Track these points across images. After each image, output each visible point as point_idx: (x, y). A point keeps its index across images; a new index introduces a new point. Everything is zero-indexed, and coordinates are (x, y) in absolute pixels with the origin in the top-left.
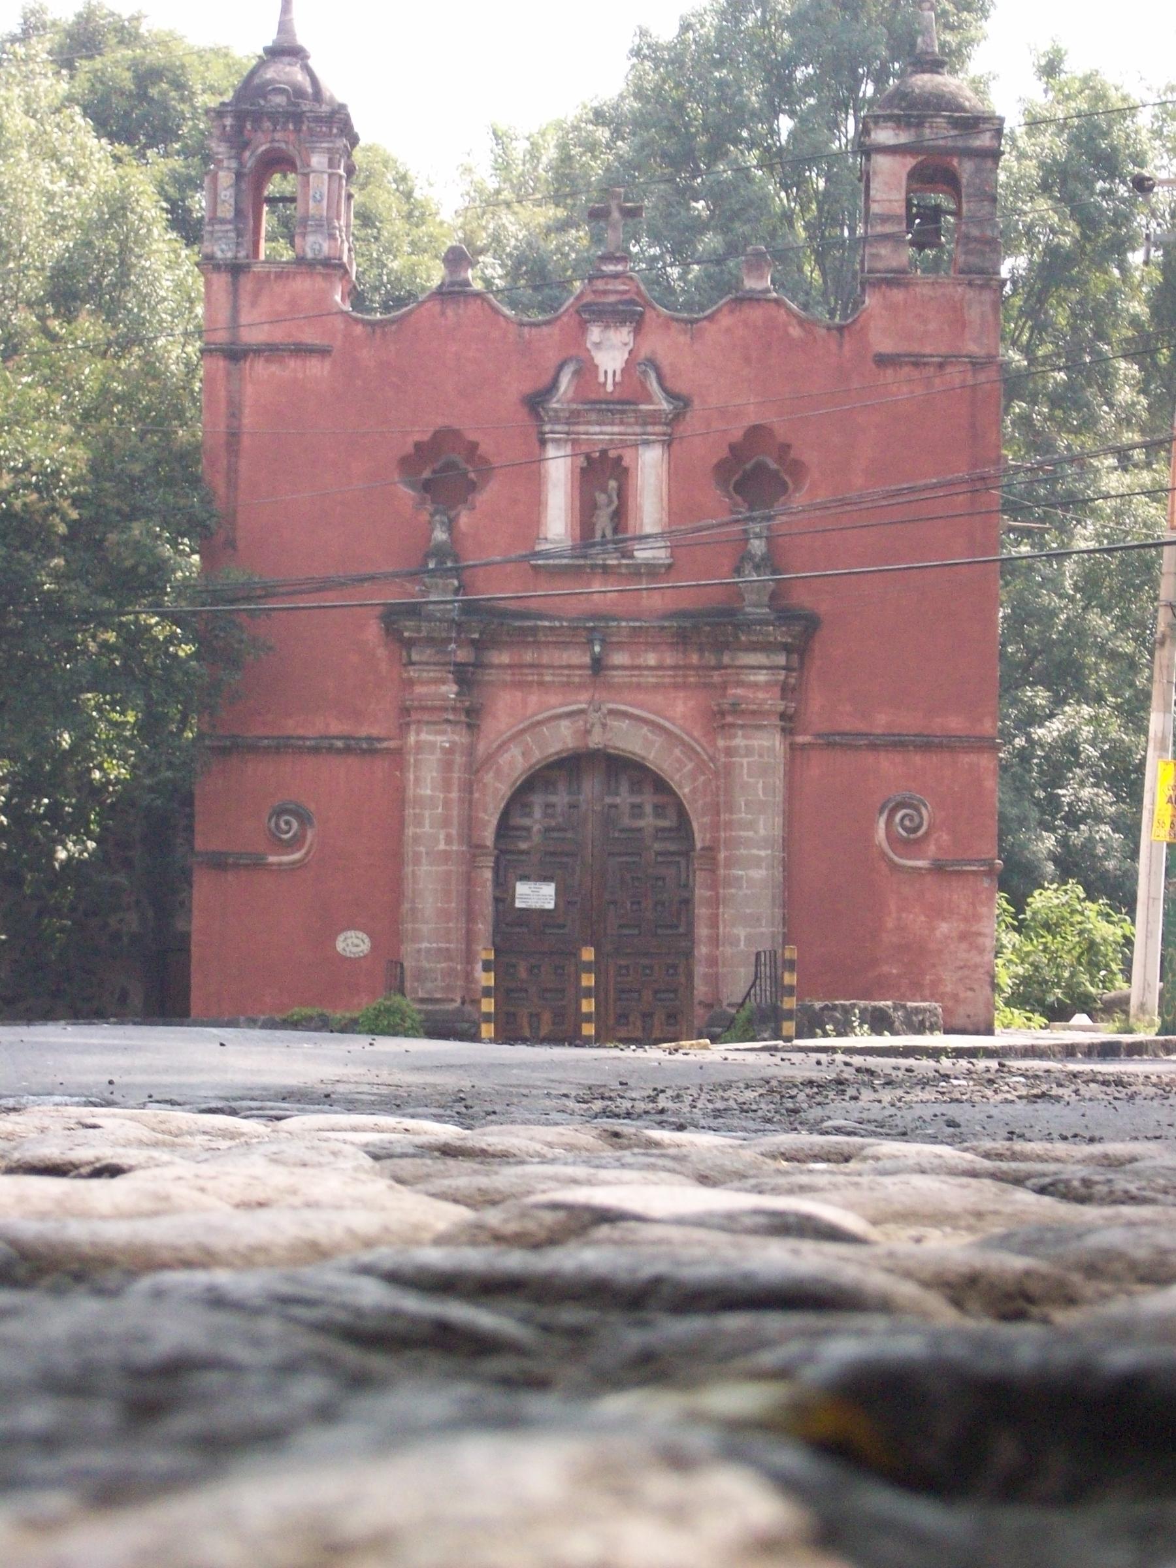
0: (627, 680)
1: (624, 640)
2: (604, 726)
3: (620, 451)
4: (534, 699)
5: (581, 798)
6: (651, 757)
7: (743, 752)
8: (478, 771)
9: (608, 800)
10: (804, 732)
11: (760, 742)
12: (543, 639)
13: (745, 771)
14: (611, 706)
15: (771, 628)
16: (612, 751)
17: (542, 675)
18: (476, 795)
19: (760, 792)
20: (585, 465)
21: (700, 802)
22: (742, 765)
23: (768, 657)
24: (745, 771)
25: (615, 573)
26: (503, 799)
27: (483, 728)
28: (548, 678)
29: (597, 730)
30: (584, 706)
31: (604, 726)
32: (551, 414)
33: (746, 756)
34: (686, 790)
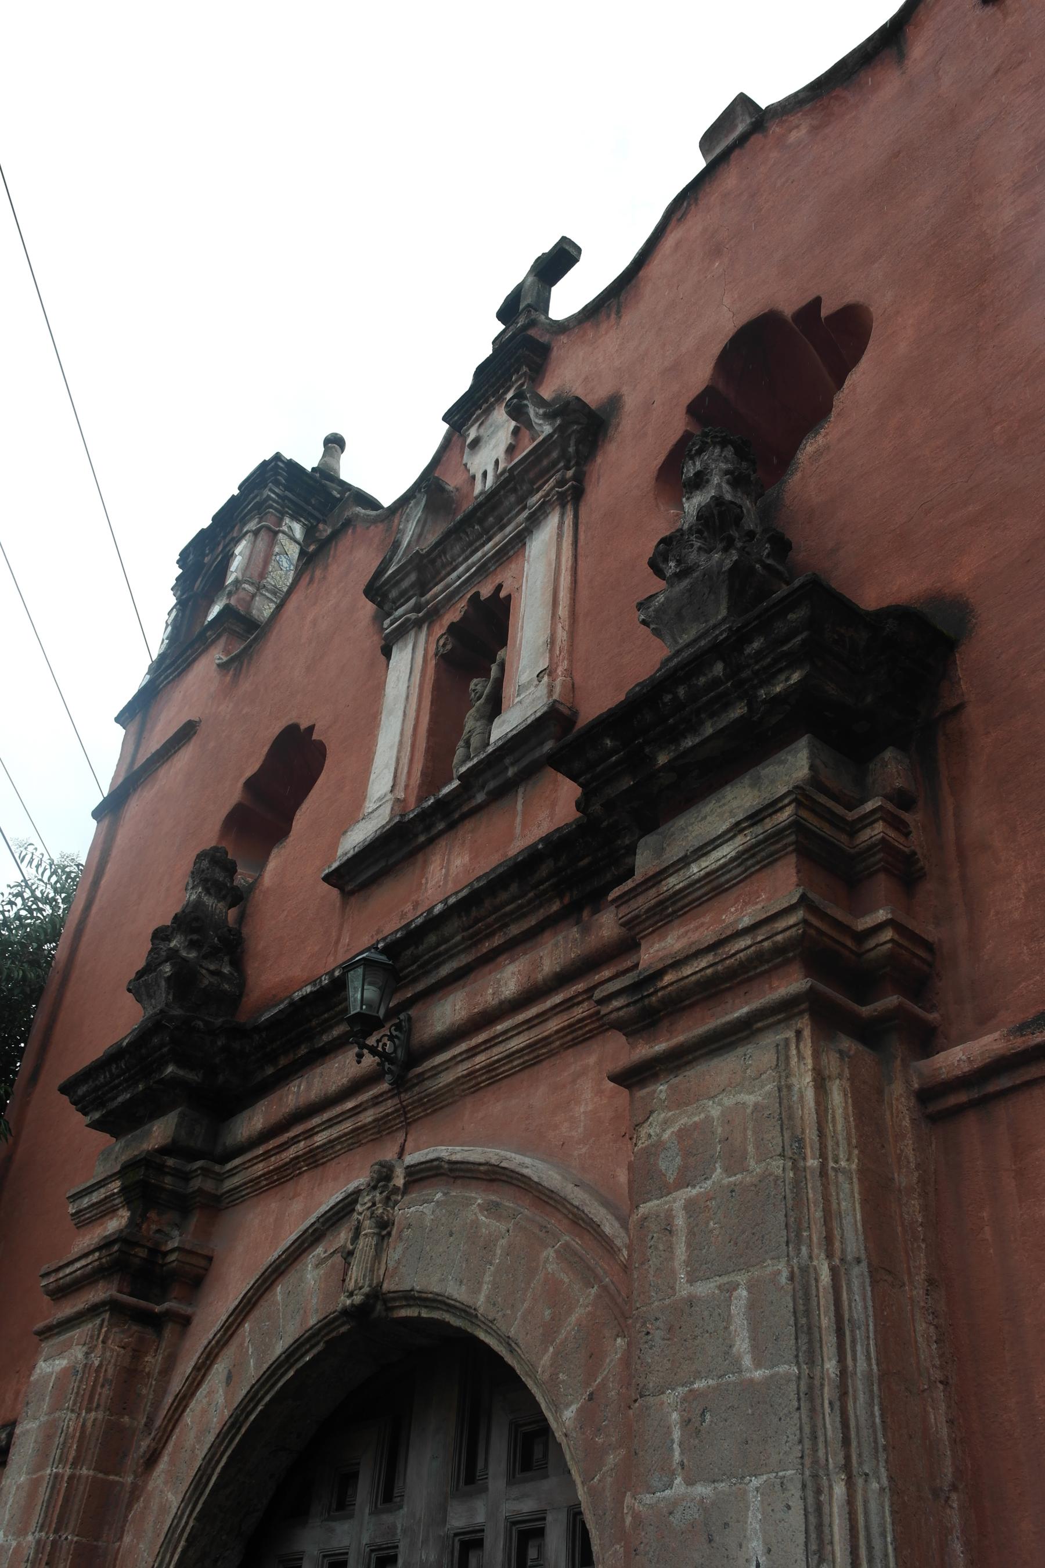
0: (461, 1070)
1: (463, 960)
2: (384, 1226)
3: (497, 582)
4: (297, 1206)
5: (399, 1519)
6: (480, 1302)
7: (669, 1166)
8: (152, 1460)
9: (458, 1520)
10: (984, 1021)
11: (729, 1101)
12: (326, 1038)
13: (681, 1251)
14: (410, 1159)
15: (718, 669)
16: (404, 1313)
17: (310, 1133)
18: (127, 1539)
19: (742, 1345)
20: (449, 647)
21: (611, 1459)
22: (669, 1230)
23: (756, 783)
24: (681, 1251)
25: (464, 817)
26: (169, 1542)
27: (195, 1321)
28: (320, 1139)
29: (366, 1244)
30: (351, 1187)
31: (384, 1226)
32: (394, 594)
33: (683, 1182)
34: (569, 1414)
